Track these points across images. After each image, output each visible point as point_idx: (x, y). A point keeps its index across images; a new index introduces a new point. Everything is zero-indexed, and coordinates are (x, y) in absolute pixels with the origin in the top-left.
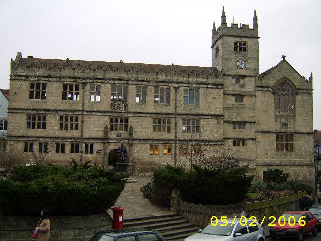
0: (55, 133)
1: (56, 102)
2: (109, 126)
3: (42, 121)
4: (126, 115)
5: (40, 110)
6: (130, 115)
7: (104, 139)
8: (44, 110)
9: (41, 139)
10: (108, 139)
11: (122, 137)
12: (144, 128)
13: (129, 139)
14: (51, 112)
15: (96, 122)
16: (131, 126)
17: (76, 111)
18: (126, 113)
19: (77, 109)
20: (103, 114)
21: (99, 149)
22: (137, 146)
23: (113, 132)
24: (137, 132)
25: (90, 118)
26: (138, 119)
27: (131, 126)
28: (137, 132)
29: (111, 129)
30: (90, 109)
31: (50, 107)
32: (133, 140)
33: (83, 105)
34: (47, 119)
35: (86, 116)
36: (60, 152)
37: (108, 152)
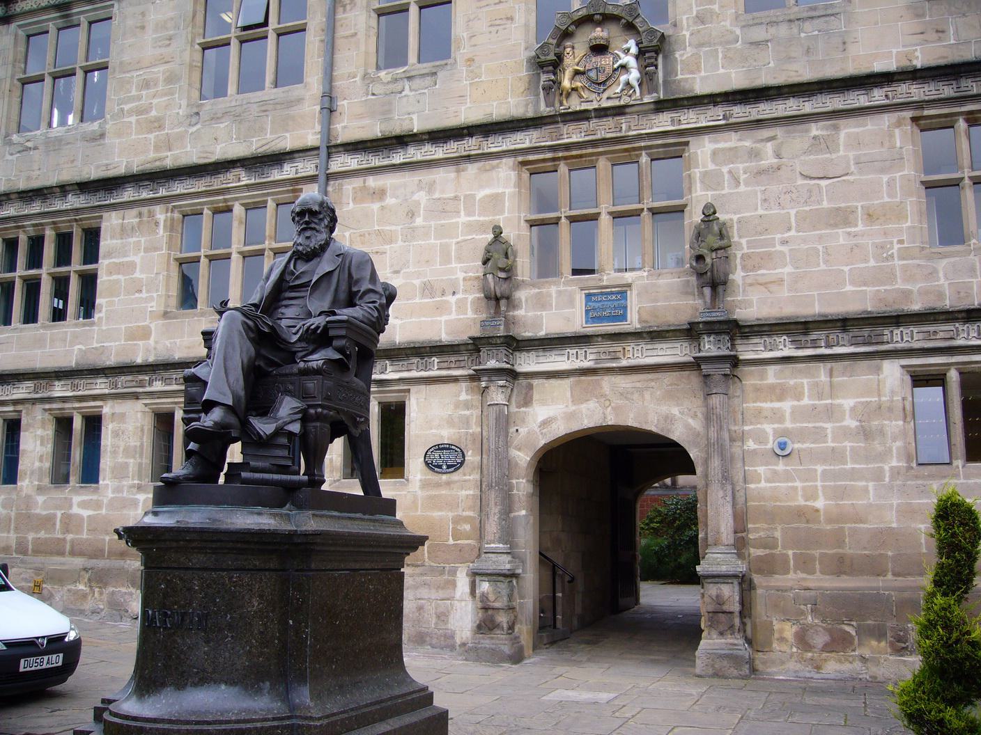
0: (145, 333)
1: (158, 124)
2: (517, 233)
3: (77, 265)
4: (663, 122)
5: (63, 189)
6: (690, 118)
7: (476, 346)
8: (85, 187)
9: (59, 389)
10: (515, 344)
11: (633, 322)
12: (842, 217)
13: (691, 332)
14: (128, 194)
15: (419, 221)
16: (709, 215)
17: (278, 158)
18: (661, 106)
19: (288, 143)
20: (471, 145)
21: (446, 435)
22: (780, 393)
23: (553, 290)
24: (768, 259)
25: (380, 194)
26: (767, 146)
27: (709, 215)
28: (768, 259)
29: (546, 268)
30: (375, 130)
31: (120, 166)
32: (735, 330)
33: (329, 109)
34: (106, 243)
35: (350, 185)
36: (74, 479)
37: (523, 458)
